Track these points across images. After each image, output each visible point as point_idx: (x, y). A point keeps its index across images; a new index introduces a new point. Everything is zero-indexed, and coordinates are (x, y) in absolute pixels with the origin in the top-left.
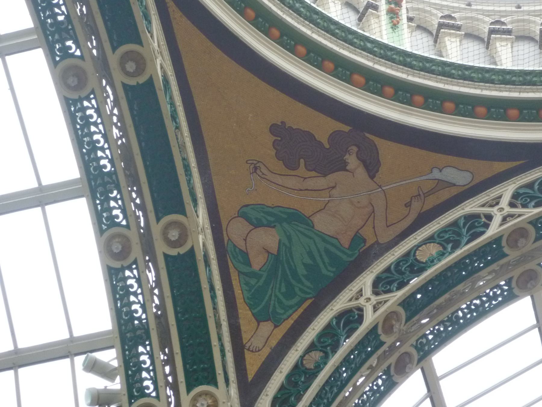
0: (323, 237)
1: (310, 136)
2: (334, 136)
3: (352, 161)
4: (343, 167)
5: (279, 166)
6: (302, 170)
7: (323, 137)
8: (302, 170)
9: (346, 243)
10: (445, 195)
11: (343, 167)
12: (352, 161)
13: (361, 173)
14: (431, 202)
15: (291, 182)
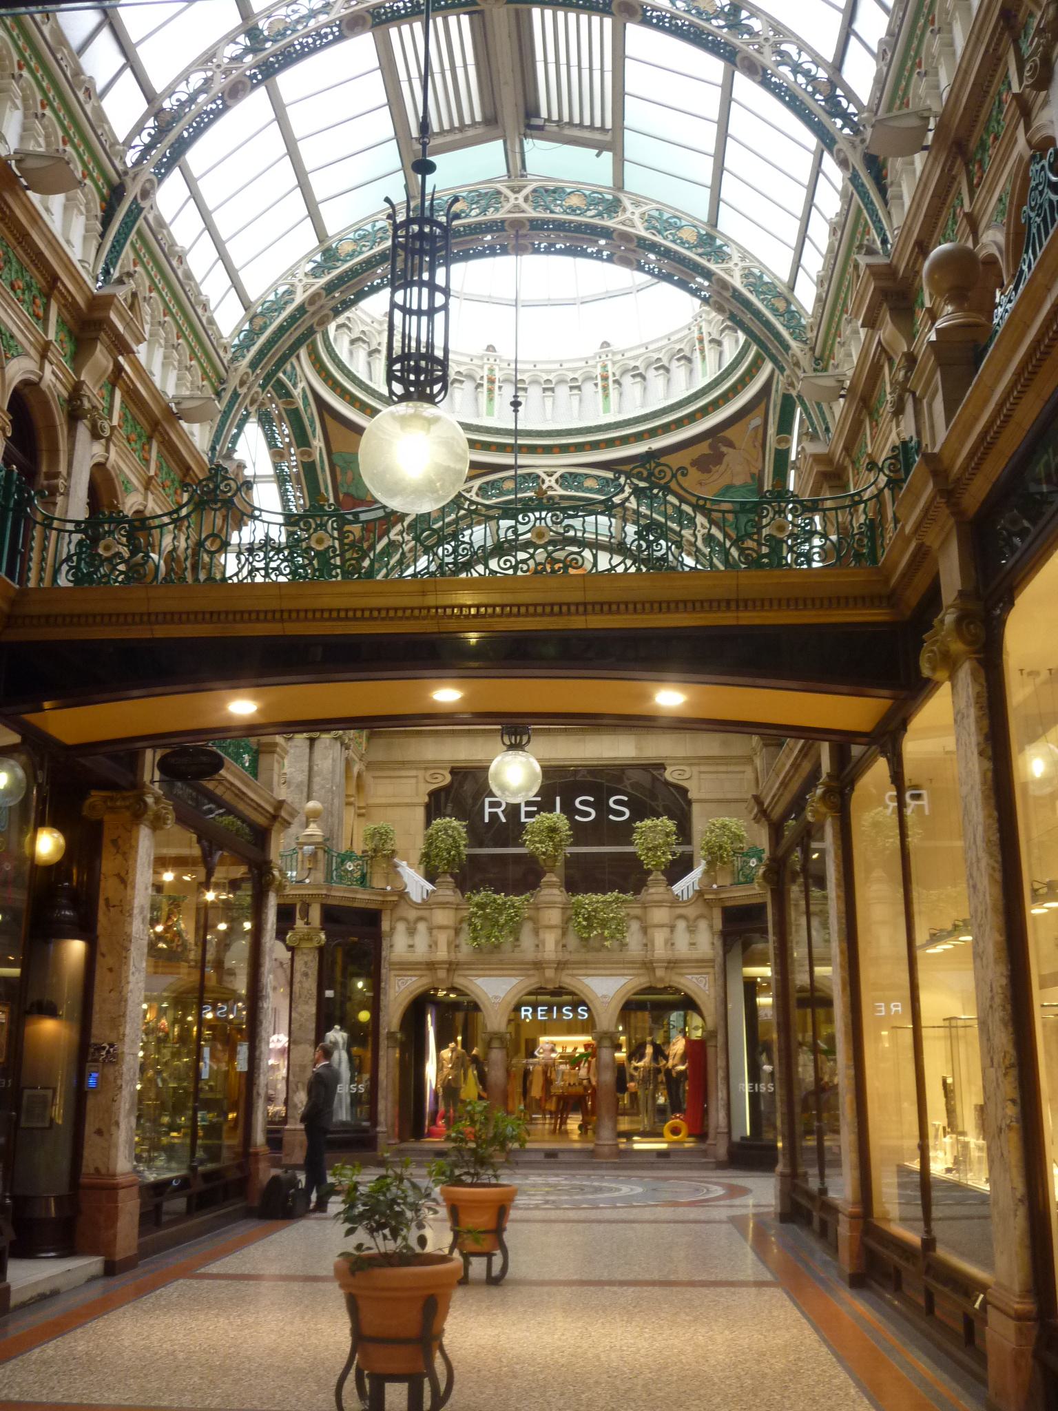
0: (743, 486)
1: (704, 455)
2: (711, 446)
3: (724, 449)
4: (723, 455)
5: (706, 476)
6: (714, 469)
7: (707, 451)
8: (714, 469)
9: (750, 481)
10: (761, 431)
11: (723, 455)
12: (724, 449)
13: (730, 450)
14: (760, 440)
15: (715, 477)
